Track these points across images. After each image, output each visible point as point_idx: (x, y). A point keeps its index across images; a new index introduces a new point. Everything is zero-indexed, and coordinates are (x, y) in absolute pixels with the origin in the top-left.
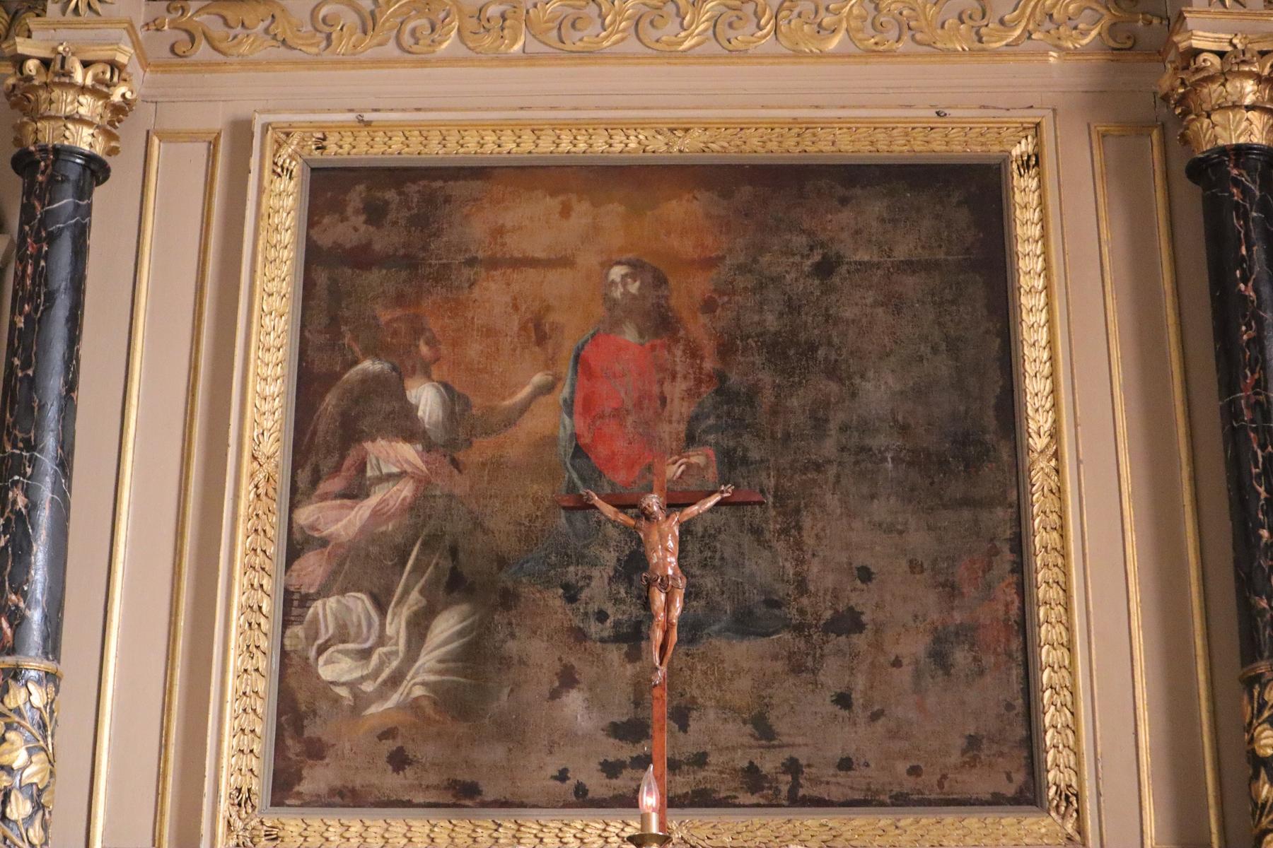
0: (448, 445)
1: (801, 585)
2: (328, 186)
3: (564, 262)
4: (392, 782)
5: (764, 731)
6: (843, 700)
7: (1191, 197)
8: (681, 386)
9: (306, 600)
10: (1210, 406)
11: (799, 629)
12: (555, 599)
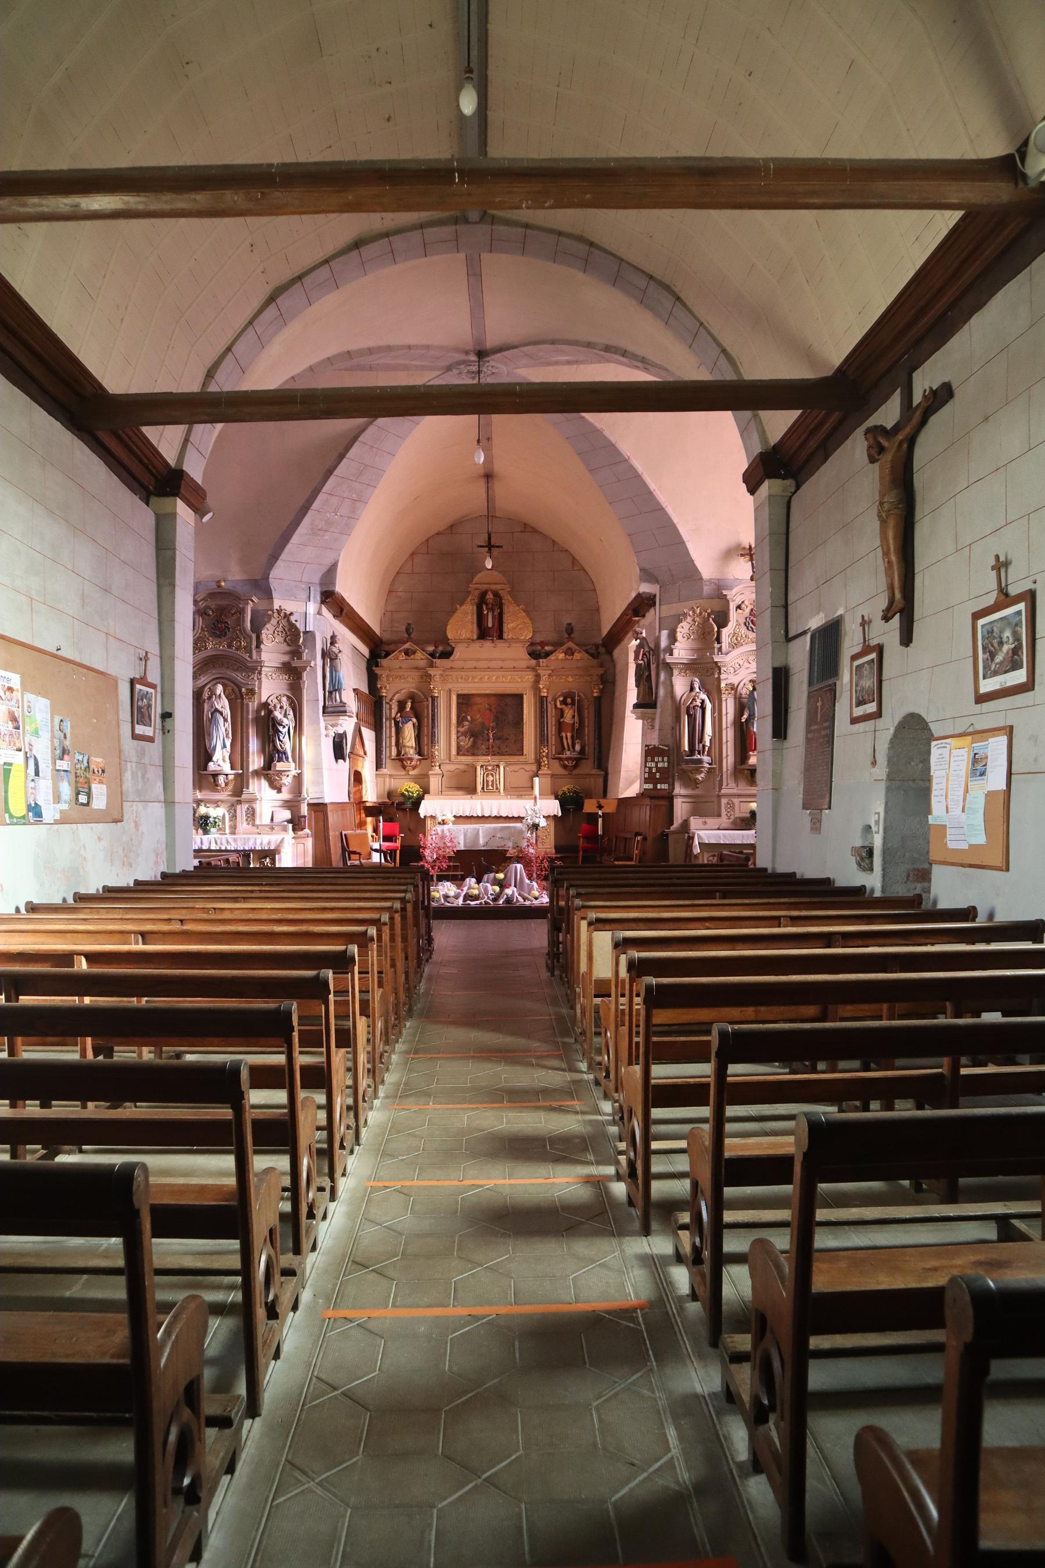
0: (471, 722)
2: (459, 696)
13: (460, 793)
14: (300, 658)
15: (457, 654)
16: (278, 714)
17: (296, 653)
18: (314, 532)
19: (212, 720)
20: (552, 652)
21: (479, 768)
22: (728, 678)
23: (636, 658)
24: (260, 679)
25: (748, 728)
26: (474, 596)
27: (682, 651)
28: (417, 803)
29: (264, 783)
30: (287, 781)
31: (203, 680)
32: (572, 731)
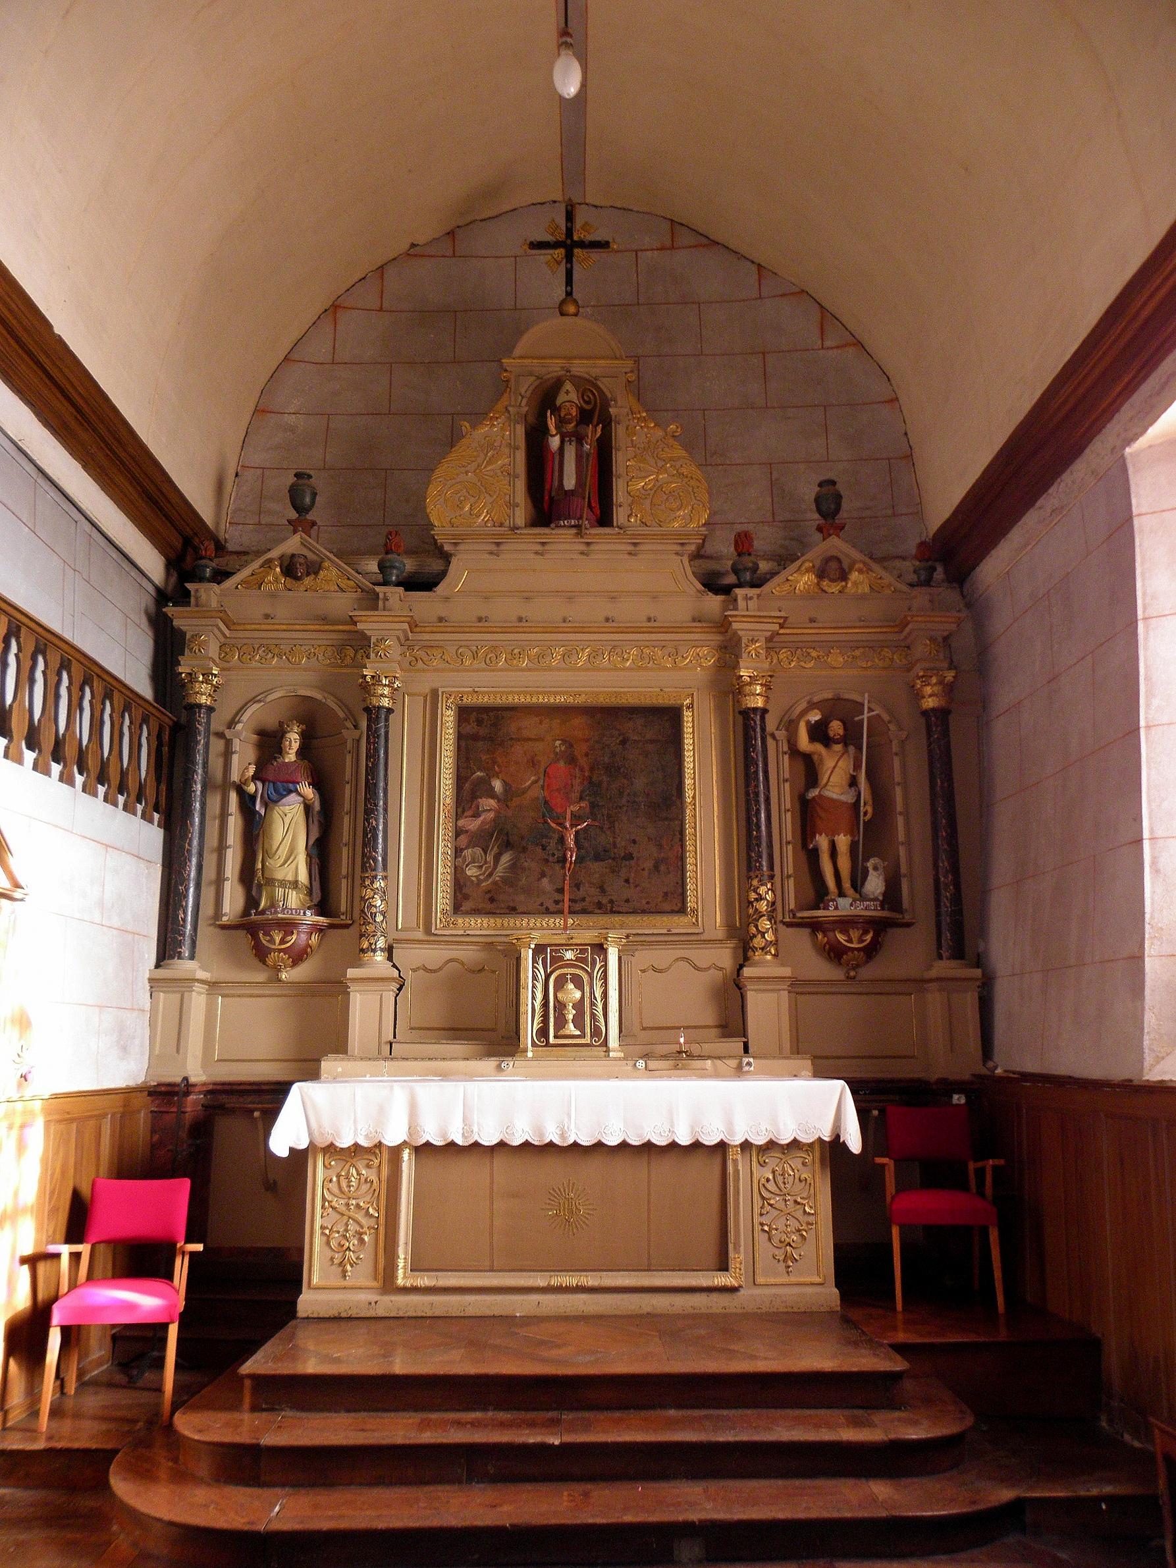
0: (506, 799)
1: (615, 846)
2: (464, 713)
3: (540, 739)
4: (489, 906)
5: (602, 890)
6: (627, 881)
7: (740, 718)
8: (578, 781)
9: (462, 850)
10: (742, 791)
11: (614, 859)
12: (539, 849)
13: (458, 1048)
15: (459, 578)
20: (773, 574)
26: (520, 401)
28: (272, 1096)
32: (853, 830)
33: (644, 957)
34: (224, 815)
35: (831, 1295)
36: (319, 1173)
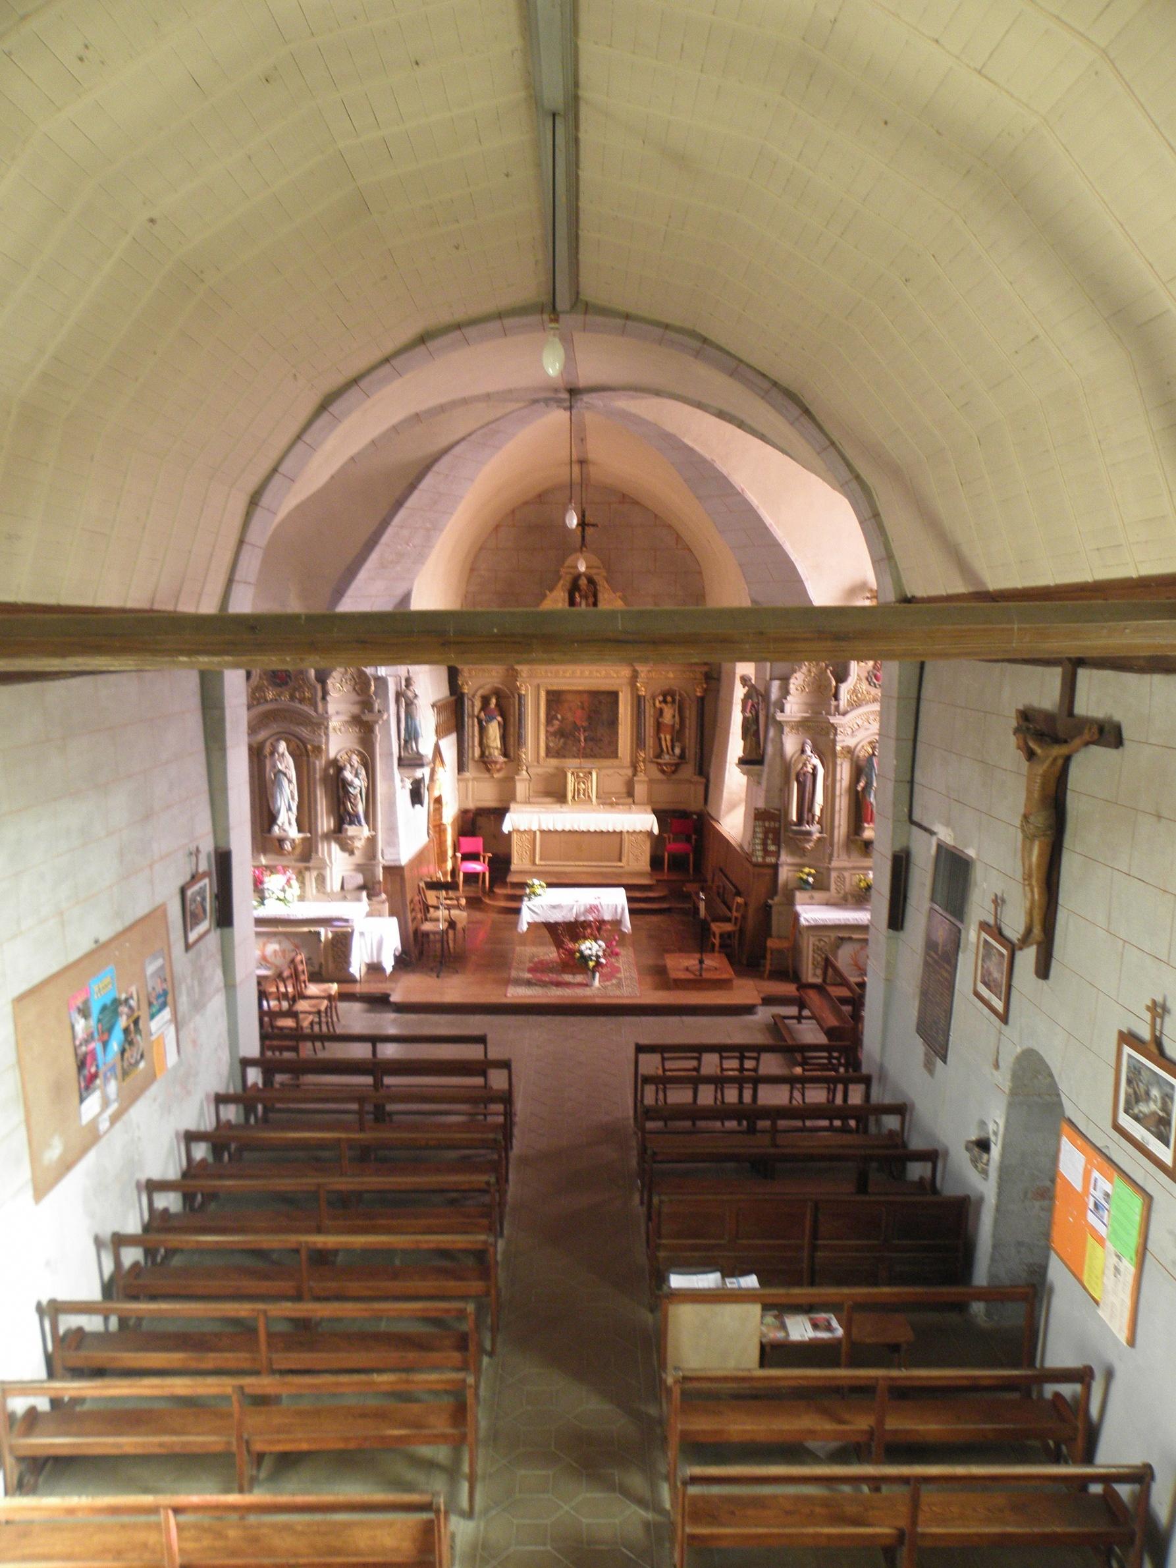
2: (548, 693)
14: (371, 710)
16: (348, 775)
17: (366, 704)
18: (383, 566)
19: (277, 783)
21: (569, 775)
22: (844, 740)
23: (744, 711)
24: (327, 735)
25: (864, 797)
27: (794, 708)
29: (335, 847)
30: (359, 844)
31: (262, 735)
33: (604, 772)
34: (473, 726)
35: (648, 868)
36: (515, 837)
